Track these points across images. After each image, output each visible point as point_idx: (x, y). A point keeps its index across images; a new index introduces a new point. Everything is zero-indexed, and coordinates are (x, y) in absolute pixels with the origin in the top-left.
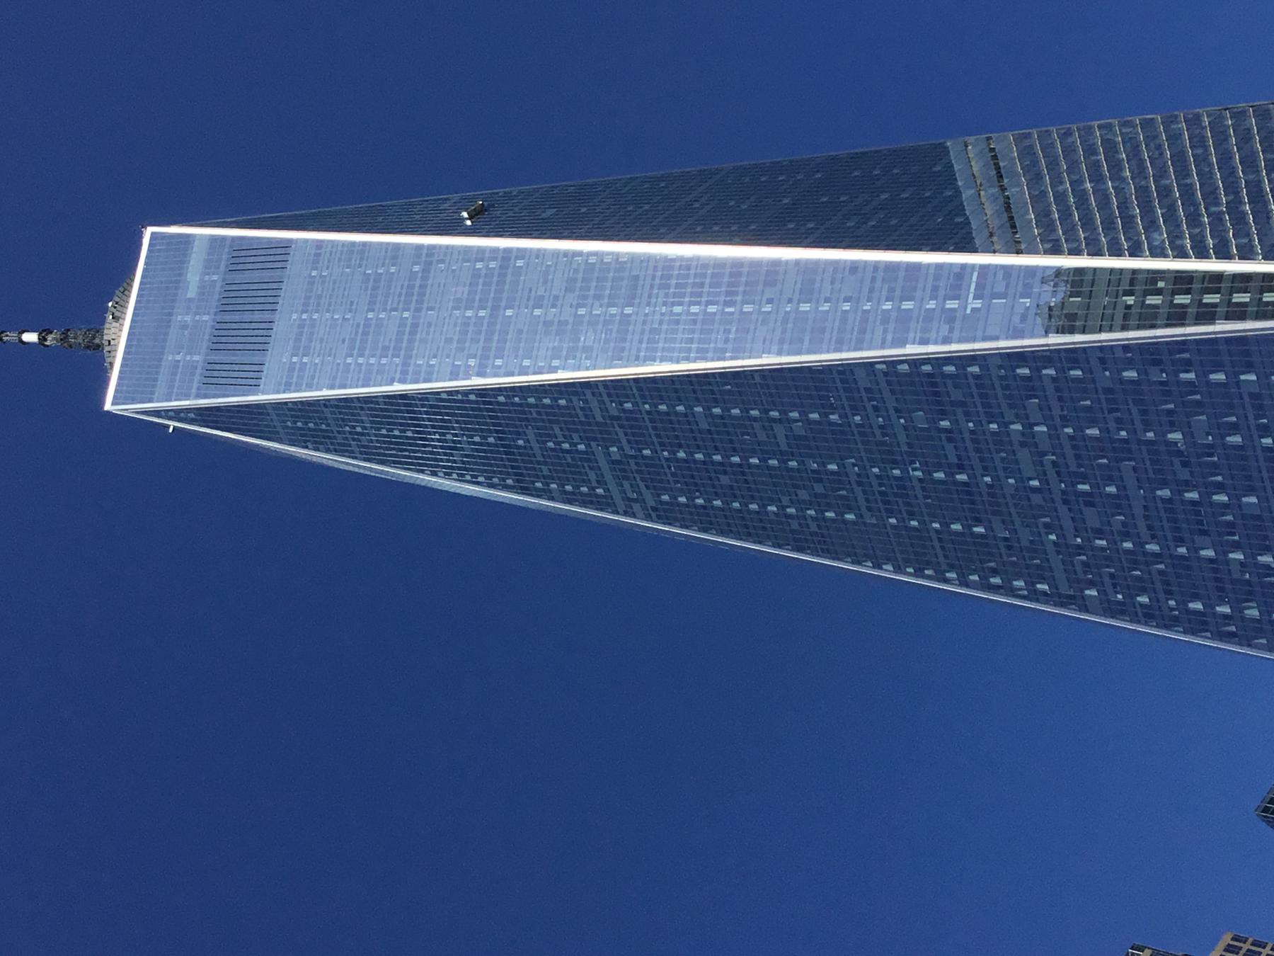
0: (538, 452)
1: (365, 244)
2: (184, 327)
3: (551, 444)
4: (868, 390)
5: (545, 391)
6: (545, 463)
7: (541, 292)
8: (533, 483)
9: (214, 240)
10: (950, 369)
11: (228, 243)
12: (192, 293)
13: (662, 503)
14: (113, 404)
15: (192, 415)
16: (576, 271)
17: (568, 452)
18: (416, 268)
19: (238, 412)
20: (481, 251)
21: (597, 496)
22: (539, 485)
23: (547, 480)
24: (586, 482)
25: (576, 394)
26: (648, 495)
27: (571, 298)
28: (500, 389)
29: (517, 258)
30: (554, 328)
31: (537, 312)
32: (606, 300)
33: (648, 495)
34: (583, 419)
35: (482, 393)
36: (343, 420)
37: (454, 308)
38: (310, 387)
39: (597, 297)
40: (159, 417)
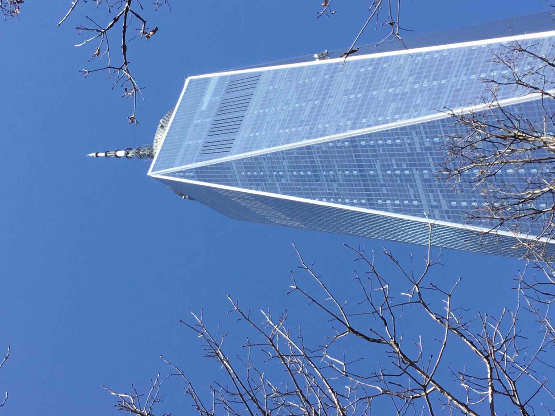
0: (381, 177)
1: (301, 67)
2: (197, 126)
3: (389, 172)
5: (389, 135)
6: (385, 186)
7: (395, 78)
8: (377, 200)
9: (221, 78)
11: (228, 79)
12: (204, 108)
13: (451, 207)
14: (153, 171)
15: (192, 174)
16: (417, 64)
17: (400, 176)
18: (327, 77)
19: (217, 168)
20: (364, 61)
21: (413, 206)
22: (380, 202)
23: (385, 197)
24: (407, 197)
25: (407, 134)
26: (443, 202)
27: (411, 79)
28: (362, 136)
29: (384, 62)
30: (399, 97)
31: (391, 90)
32: (432, 78)
33: (443, 202)
34: (409, 151)
35: (352, 140)
36: (273, 167)
37: (344, 95)
38: (258, 148)
39: (426, 77)
40: (175, 176)
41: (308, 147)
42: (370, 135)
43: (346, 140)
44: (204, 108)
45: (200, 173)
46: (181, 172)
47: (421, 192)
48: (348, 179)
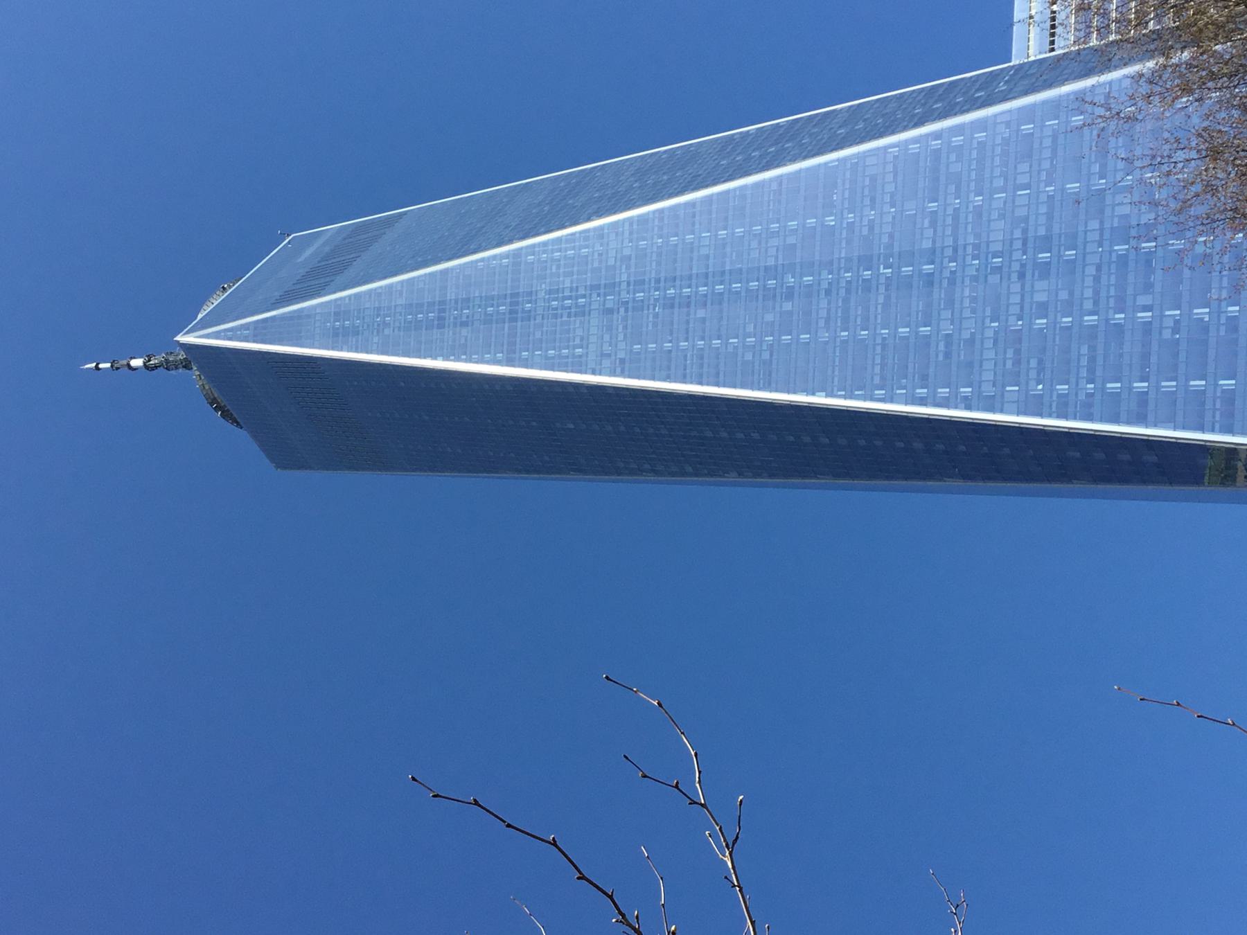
4: (873, 179)
10: (957, 140)
26: (622, 345)
33: (622, 345)
35: (517, 254)
42: (545, 244)
43: (506, 255)
47: (593, 330)
48: (488, 320)
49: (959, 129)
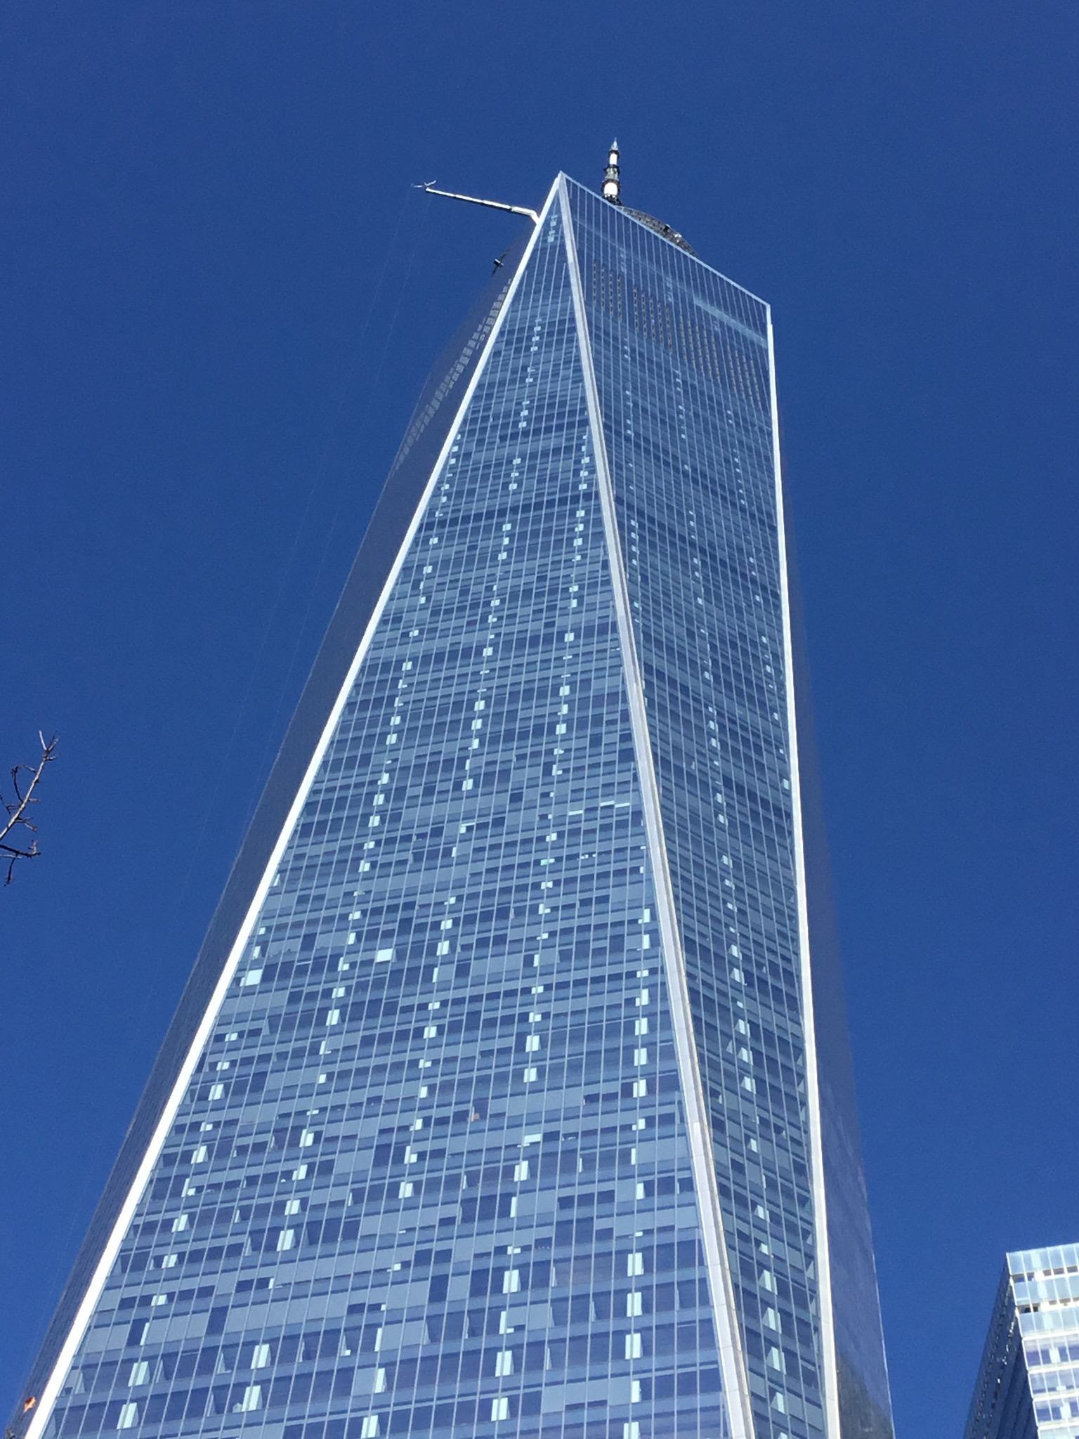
2: (660, 279)
10: (643, 998)
12: (698, 302)
15: (551, 239)
29: (766, 600)
41: (585, 423)
43: (592, 482)
44: (698, 302)
45: (550, 255)
46: (559, 221)
49: (659, 991)
